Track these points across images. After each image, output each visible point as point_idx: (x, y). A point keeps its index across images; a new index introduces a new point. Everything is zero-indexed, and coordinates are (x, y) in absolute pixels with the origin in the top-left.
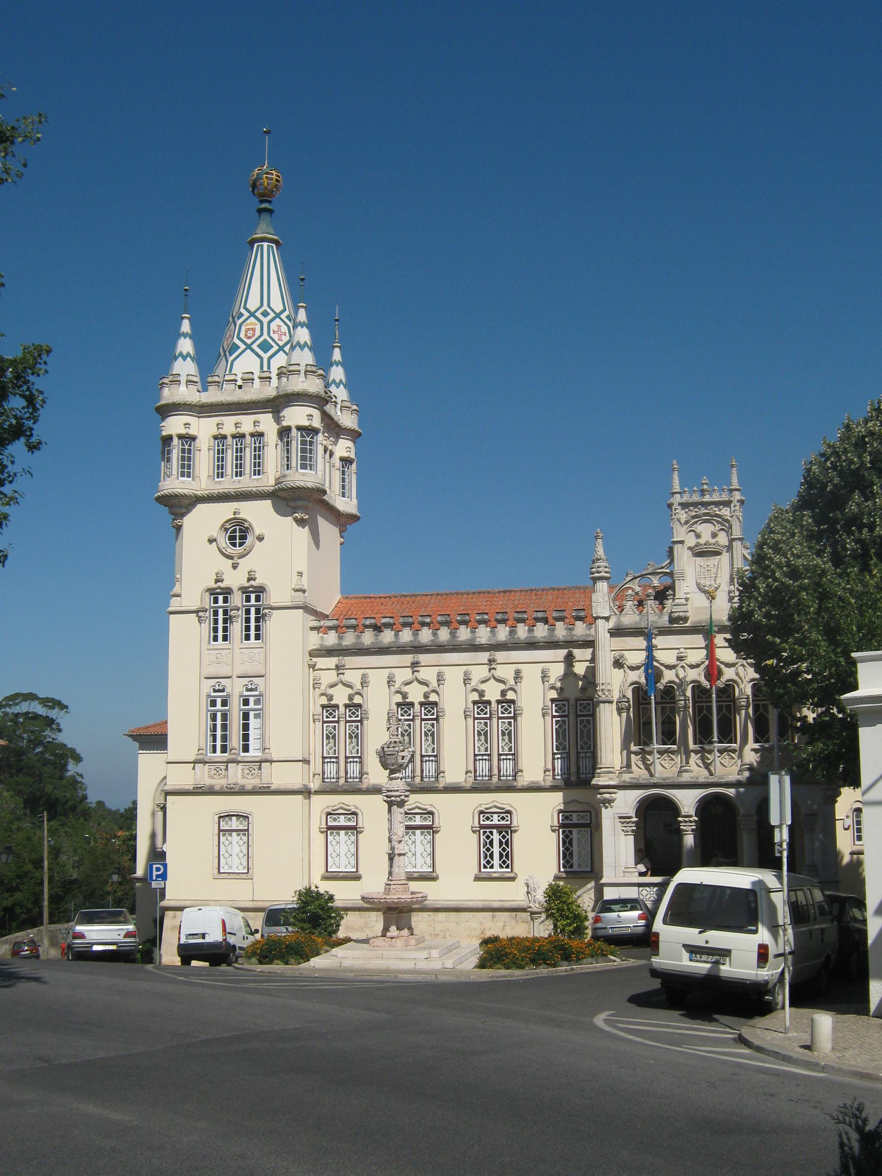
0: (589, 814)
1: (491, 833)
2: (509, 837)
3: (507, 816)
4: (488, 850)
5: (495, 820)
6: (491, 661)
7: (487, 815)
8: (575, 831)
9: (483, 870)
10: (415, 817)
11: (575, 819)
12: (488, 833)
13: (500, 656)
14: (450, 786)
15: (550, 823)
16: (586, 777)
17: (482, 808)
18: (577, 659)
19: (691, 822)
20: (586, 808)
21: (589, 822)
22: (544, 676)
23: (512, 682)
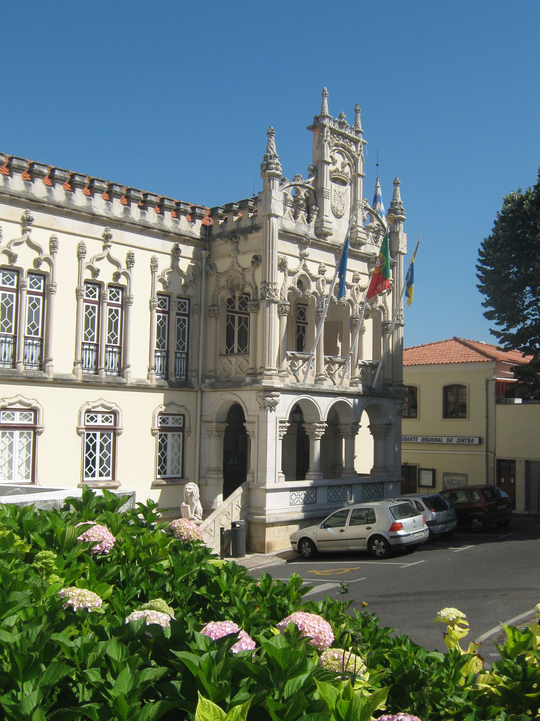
0: (182, 417)
1: (95, 435)
2: (112, 440)
3: (111, 417)
4: (105, 455)
5: (100, 421)
6: (107, 237)
7: (91, 415)
8: (170, 434)
9: (85, 479)
10: (14, 414)
11: (171, 423)
12: (91, 436)
13: (117, 234)
14: (60, 377)
15: (150, 426)
16: (181, 379)
17: (89, 407)
18: (182, 254)
19: (323, 427)
20: (182, 411)
21: (181, 425)
22: (154, 266)
23: (124, 266)
